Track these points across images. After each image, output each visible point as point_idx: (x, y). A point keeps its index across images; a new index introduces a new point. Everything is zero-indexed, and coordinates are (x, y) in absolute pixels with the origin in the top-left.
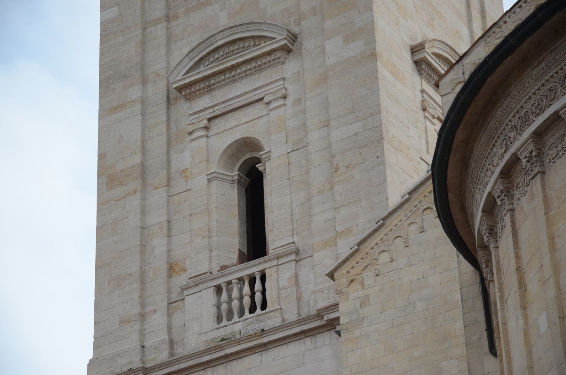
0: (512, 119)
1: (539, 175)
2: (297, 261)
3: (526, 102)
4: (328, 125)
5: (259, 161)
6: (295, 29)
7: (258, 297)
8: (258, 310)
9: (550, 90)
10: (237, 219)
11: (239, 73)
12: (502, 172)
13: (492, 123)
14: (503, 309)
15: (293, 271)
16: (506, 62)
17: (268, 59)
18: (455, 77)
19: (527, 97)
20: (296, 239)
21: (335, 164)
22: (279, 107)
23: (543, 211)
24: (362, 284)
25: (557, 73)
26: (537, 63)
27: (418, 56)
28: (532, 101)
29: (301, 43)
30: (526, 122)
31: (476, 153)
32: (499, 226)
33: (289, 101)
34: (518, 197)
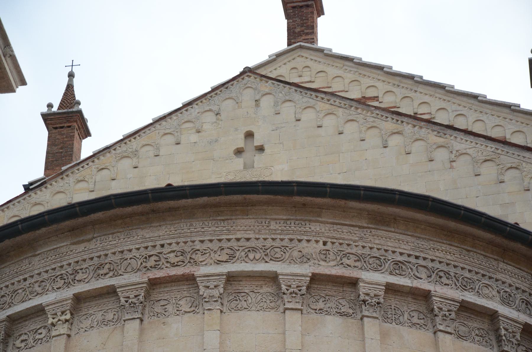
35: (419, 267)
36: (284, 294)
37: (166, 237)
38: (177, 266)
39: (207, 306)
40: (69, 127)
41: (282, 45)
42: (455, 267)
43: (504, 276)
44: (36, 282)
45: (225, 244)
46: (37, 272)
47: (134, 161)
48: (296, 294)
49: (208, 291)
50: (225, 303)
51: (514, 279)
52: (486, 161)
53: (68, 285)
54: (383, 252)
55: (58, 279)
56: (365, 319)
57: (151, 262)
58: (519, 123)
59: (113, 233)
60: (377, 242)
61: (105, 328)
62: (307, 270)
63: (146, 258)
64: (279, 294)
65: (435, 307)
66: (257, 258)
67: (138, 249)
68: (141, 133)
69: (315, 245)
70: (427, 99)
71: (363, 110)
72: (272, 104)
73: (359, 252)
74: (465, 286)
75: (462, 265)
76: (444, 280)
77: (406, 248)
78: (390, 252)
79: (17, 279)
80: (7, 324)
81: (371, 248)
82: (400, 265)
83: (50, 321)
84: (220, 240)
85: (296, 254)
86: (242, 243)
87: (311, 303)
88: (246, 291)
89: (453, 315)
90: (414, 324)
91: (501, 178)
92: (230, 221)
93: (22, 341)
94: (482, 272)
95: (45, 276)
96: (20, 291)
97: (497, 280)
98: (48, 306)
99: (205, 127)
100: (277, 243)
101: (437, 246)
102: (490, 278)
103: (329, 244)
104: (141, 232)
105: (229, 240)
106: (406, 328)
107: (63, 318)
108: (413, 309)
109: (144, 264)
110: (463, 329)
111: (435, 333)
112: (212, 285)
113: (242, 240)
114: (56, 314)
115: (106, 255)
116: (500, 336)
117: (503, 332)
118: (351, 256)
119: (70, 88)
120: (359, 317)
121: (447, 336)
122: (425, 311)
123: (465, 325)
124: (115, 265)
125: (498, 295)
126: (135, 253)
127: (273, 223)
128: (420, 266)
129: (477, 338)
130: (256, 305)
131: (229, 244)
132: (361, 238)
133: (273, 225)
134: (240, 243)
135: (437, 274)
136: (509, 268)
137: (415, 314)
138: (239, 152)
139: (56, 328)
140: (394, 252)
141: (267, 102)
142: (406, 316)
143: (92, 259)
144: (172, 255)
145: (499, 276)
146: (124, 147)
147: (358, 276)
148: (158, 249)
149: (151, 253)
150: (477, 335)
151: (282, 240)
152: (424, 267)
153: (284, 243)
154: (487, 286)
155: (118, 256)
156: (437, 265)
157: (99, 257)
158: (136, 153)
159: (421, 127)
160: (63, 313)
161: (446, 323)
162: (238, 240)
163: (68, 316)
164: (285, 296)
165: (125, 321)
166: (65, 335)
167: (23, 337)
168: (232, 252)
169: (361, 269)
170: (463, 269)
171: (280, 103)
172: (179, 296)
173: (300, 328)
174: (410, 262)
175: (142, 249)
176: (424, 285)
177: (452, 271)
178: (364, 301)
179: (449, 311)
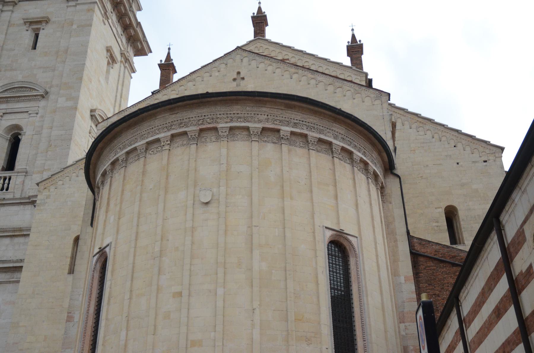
0: (120, 145)
1: (124, 167)
2: (25, 176)
3: (126, 140)
4: (52, 129)
5: (20, 134)
6: (48, 90)
7: (6, 185)
8: (4, 191)
9: (136, 139)
10: (5, 154)
11: (21, 100)
12: (111, 163)
13: (113, 144)
14: (99, 211)
15: (23, 179)
16: (123, 124)
17: (34, 98)
18: (104, 125)
19: (127, 139)
20: (27, 168)
21: (50, 143)
22: (34, 117)
23: (122, 180)
24: (49, 190)
25: (140, 133)
26: (134, 128)
27: (93, 114)
28: (129, 141)
29: (49, 96)
30: (124, 147)
31: (104, 153)
32: (106, 182)
33: (38, 116)
34: (115, 173)
35: (303, 125)
36: (252, 135)
37: (206, 112)
38: (211, 123)
39: (222, 139)
40: (168, 69)
41: (252, 37)
42: (317, 125)
43: (335, 128)
44: (156, 129)
45: (229, 116)
46: (157, 125)
47: (194, 83)
48: (256, 135)
49: (222, 133)
50: (229, 138)
51: (338, 130)
52: (329, 84)
53: (169, 130)
54: (290, 119)
55: (165, 128)
56: (283, 145)
57: (201, 122)
58: (342, 70)
59: (185, 111)
60: (287, 115)
61: (183, 147)
62: (260, 126)
63: (198, 120)
64: (250, 135)
65: (309, 140)
66: (241, 121)
67: (195, 117)
68: (196, 72)
69: (264, 116)
70: (308, 60)
71: (283, 64)
72: (248, 61)
73: (281, 119)
74: (320, 132)
75: (319, 124)
76: (313, 130)
77: (299, 118)
78: (292, 119)
79: (149, 128)
80: (146, 145)
81: (285, 118)
82: (296, 124)
83: (162, 144)
84: (227, 114)
85: (256, 119)
86: (236, 115)
87: (262, 138)
88: (237, 134)
89: (316, 143)
90: (301, 147)
91: (335, 91)
92: (231, 106)
93: (152, 151)
94: (327, 127)
95: (160, 127)
96: (151, 133)
97: (332, 130)
98: (161, 138)
99: (222, 70)
100: (249, 115)
101: (311, 117)
102: (330, 129)
103: (269, 116)
104: (196, 110)
105: (230, 114)
106: (298, 148)
107: (167, 143)
108: (301, 141)
109: (198, 123)
110: (319, 148)
111: (309, 150)
112: (224, 131)
113: (236, 114)
114: (164, 141)
115: (183, 119)
116: (333, 151)
117: (334, 150)
118: (278, 120)
119: (169, 54)
120: (280, 144)
121: (313, 151)
122: (305, 142)
123: (320, 147)
124: (187, 123)
125: (332, 136)
126: (194, 119)
127: (247, 107)
128: (304, 124)
129: (324, 152)
130: (241, 139)
131: (231, 116)
132: (281, 114)
133: (248, 108)
134: (235, 115)
135: (310, 128)
136: (337, 125)
137: (301, 143)
138: (235, 80)
139: (164, 147)
140: (294, 119)
141: (245, 60)
142: (298, 143)
143: (178, 120)
144: (208, 119)
145: (333, 129)
146: (190, 77)
147: (280, 128)
148: (203, 117)
149: (200, 119)
150: (324, 151)
151: (251, 114)
152: (305, 125)
153: (252, 115)
154: (329, 132)
155: (188, 120)
156: (310, 124)
157: (180, 120)
158: (194, 80)
159: (305, 71)
160: (167, 141)
161: (313, 146)
162: (234, 114)
163: (169, 142)
164: (252, 136)
165: (190, 144)
166: (168, 150)
167: (152, 150)
168: (232, 119)
169: (281, 125)
170: (320, 126)
171: (251, 61)
172: (211, 135)
173: (258, 148)
174: (300, 123)
175: (197, 117)
176: (305, 132)
177: (316, 126)
178: (282, 138)
179: (314, 141)
